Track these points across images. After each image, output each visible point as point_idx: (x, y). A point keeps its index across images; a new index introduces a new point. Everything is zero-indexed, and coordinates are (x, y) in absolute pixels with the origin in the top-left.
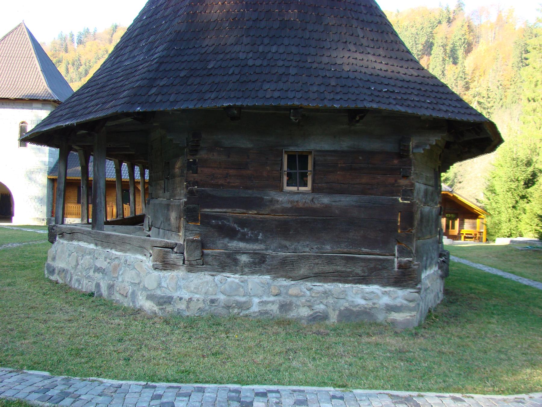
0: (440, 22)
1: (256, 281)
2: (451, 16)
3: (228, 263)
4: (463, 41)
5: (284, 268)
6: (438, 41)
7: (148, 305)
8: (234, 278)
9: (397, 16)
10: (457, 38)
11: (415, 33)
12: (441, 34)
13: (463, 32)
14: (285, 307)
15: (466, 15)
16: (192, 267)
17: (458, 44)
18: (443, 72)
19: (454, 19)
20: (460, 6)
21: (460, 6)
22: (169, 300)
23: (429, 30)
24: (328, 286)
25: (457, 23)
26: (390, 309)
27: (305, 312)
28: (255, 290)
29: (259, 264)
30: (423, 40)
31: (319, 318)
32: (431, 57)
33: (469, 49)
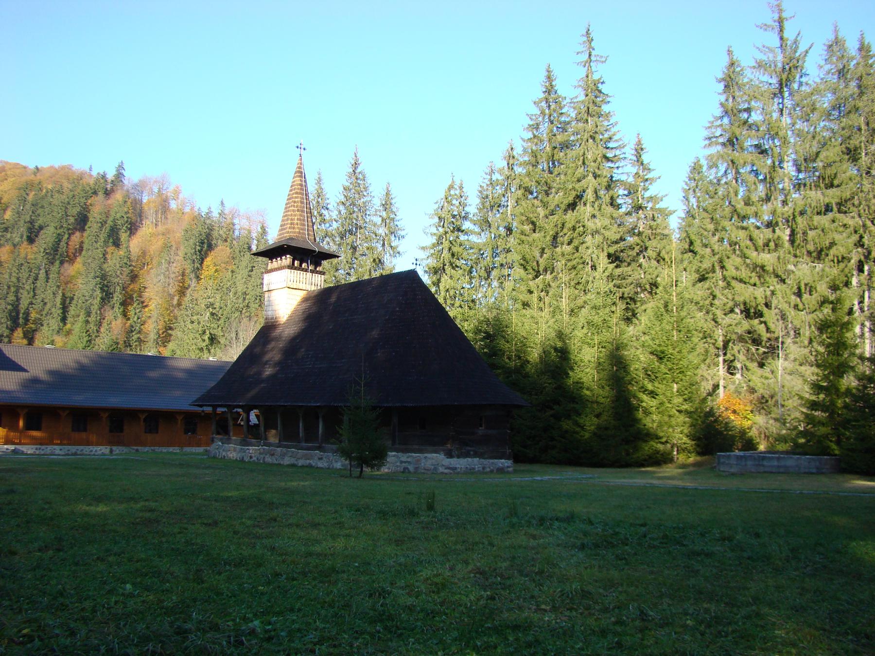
0: (95, 193)
1: (476, 460)
2: (109, 187)
3: (467, 455)
4: (126, 219)
5: (481, 456)
6: (95, 214)
7: (446, 471)
8: (470, 459)
9: (35, 174)
10: (118, 215)
11: (66, 201)
12: (97, 207)
13: (126, 210)
14: (484, 468)
15: (125, 188)
16: (458, 457)
17: (119, 222)
18: (104, 255)
19: (112, 191)
20: (119, 176)
21: (119, 176)
22: (456, 468)
23: (83, 200)
24: (491, 461)
25: (118, 196)
26: (508, 467)
27: (488, 470)
28: (475, 463)
29: (476, 455)
30: (74, 211)
31: (492, 471)
32: (85, 234)
33: (133, 228)
